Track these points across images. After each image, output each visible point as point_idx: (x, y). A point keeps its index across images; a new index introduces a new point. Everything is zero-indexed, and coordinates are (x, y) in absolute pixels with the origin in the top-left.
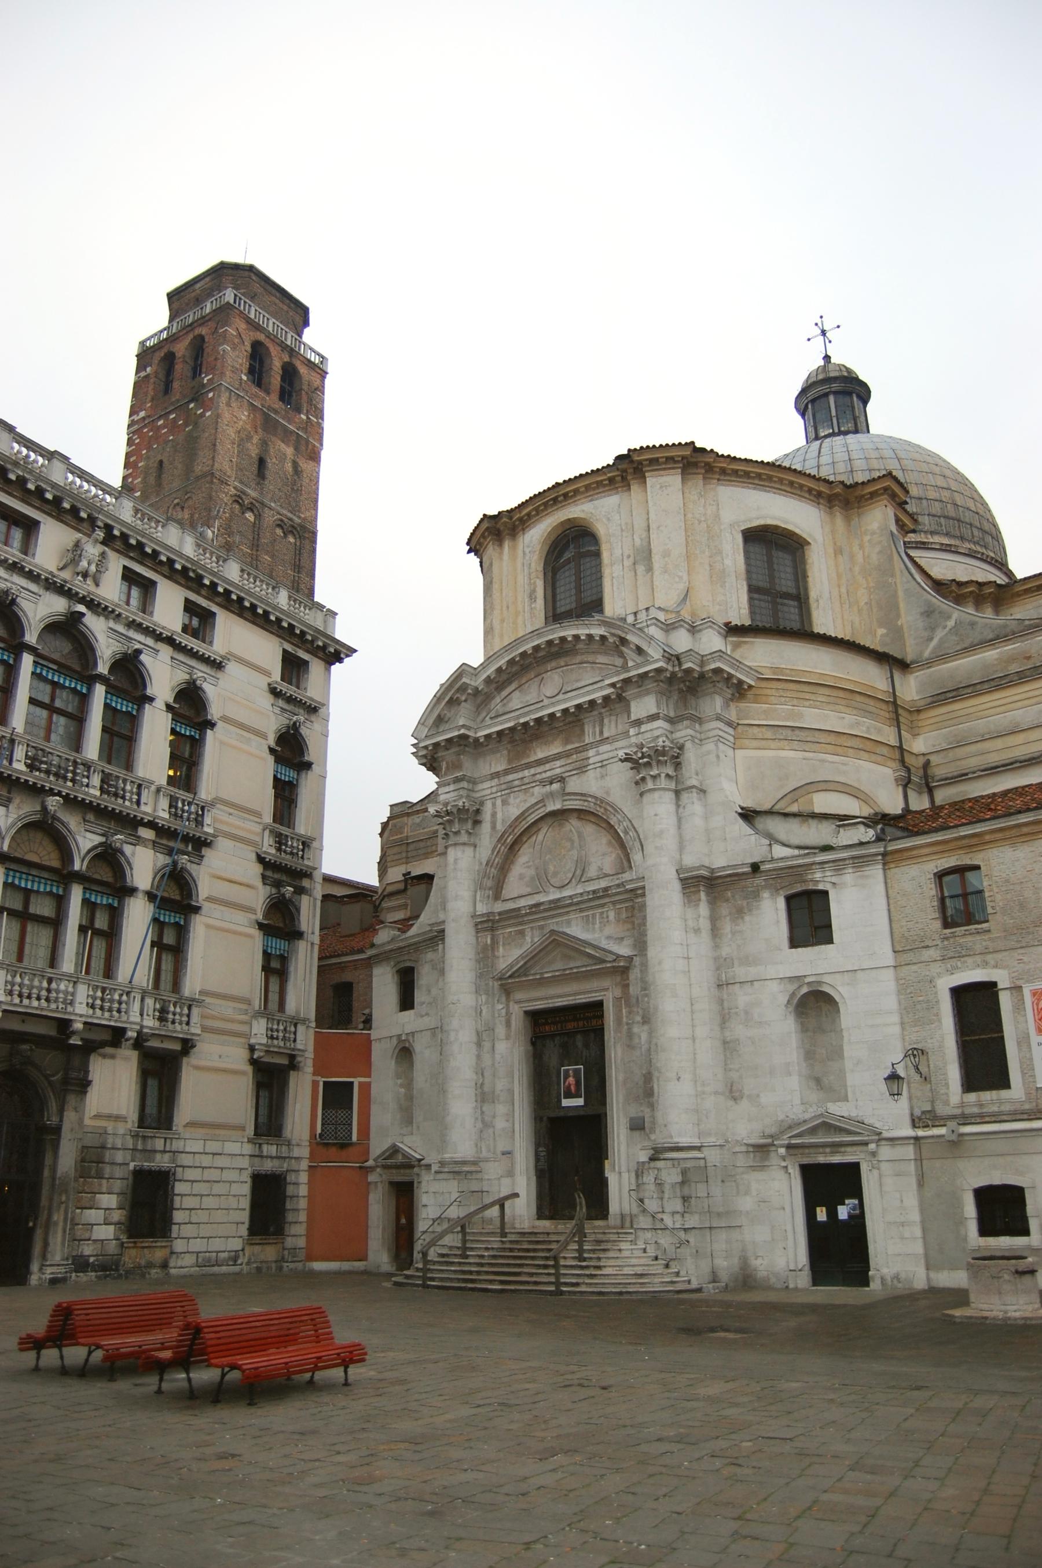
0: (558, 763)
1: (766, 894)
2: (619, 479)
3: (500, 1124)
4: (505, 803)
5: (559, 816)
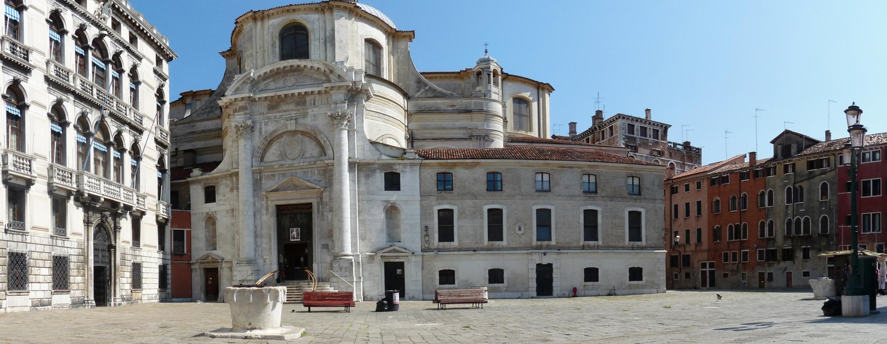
0: (293, 112)
1: (378, 171)
2: (320, 9)
3: (264, 246)
4: (266, 124)
5: (295, 132)
